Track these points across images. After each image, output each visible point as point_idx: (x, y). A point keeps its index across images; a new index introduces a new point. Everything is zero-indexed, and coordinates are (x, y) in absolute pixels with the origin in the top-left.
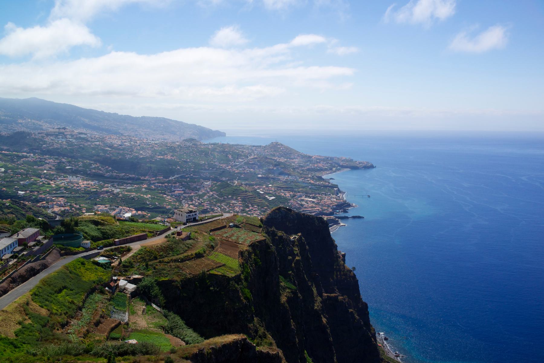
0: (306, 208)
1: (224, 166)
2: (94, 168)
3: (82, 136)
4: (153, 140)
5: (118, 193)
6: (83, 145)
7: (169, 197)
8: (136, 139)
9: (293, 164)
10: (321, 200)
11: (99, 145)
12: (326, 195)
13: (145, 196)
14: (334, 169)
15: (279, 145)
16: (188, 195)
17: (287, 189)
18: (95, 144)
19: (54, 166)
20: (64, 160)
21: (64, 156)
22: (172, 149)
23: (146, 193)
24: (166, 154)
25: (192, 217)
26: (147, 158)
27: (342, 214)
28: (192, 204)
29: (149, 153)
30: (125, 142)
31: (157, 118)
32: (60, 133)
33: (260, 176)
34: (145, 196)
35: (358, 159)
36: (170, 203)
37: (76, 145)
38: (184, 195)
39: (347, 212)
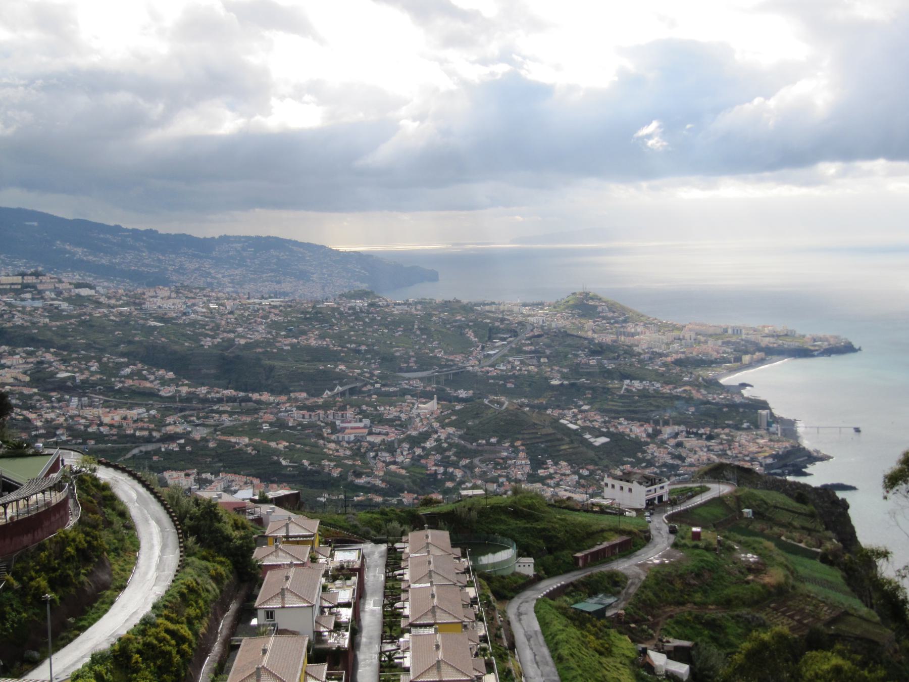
1: (458, 358)
2: (130, 376)
3: (85, 292)
4: (263, 298)
5: (204, 440)
6: (90, 314)
7: (333, 446)
8: (220, 294)
10: (730, 442)
11: (131, 313)
13: (273, 444)
14: (746, 359)
15: (592, 298)
17: (633, 415)
18: (121, 314)
19: (25, 373)
20: (49, 357)
21: (47, 345)
22: (316, 316)
23: (271, 436)
24: (304, 333)
26: (257, 344)
28: (395, 463)
29: (260, 333)
30: (194, 305)
32: (25, 287)
33: (555, 382)
34: (273, 444)
35: (807, 330)
36: (338, 461)
37: (70, 317)
38: (369, 438)
39: (805, 474)
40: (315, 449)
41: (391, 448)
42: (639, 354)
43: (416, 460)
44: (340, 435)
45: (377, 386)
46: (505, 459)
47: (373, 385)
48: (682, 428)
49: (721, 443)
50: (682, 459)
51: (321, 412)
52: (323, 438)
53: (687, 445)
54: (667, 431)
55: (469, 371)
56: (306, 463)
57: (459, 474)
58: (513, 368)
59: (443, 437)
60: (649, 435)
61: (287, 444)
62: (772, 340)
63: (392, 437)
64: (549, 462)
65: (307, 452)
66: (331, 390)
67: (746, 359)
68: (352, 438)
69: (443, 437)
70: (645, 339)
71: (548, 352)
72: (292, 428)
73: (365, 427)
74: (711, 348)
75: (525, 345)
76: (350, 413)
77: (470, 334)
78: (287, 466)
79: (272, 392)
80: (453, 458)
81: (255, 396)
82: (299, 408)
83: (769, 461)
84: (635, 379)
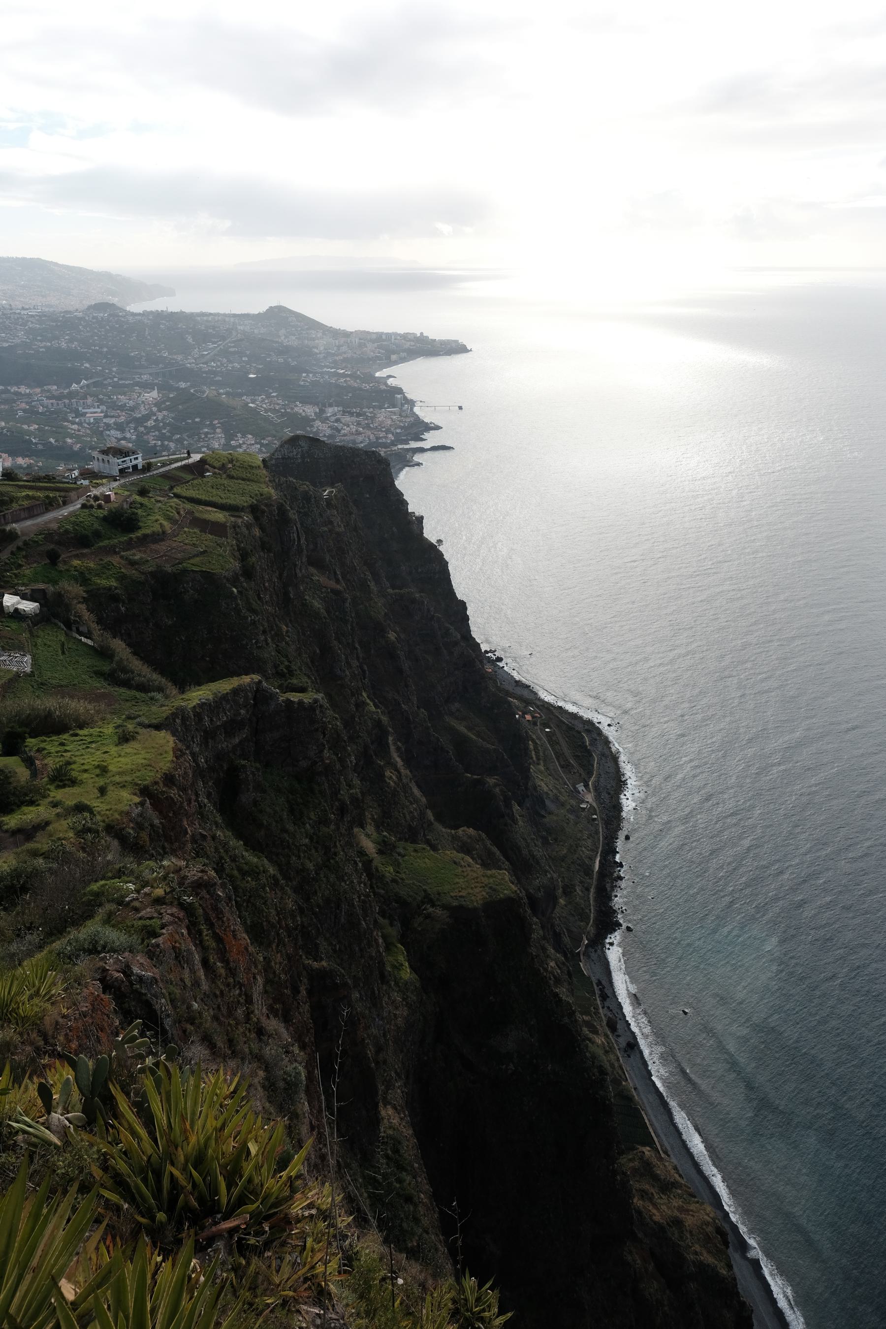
0: (345, 435)
1: (179, 357)
7: (75, 427)
9: (315, 350)
10: (373, 418)
12: (381, 408)
13: (25, 427)
14: (394, 357)
16: (113, 420)
25: (130, 465)
27: (414, 445)
28: (124, 438)
31: (24, 259)
34: (25, 427)
36: (78, 438)
38: (105, 420)
40: (60, 430)
41: (120, 427)
42: (317, 354)
43: (140, 436)
44: (82, 419)
45: (116, 379)
46: (206, 434)
47: (112, 379)
48: (340, 408)
49: (367, 419)
50: (339, 431)
51: (67, 401)
52: (68, 421)
53: (343, 421)
54: (330, 411)
55: (187, 368)
56: (52, 440)
57: (172, 445)
58: (222, 365)
59: (160, 418)
60: (316, 413)
61: (37, 427)
62: (412, 343)
63: (122, 419)
64: (239, 435)
65: (53, 432)
66: (78, 383)
67: (394, 357)
68: (92, 420)
69: (160, 418)
70: (322, 344)
71: (248, 352)
72: (41, 414)
73: (102, 412)
74: (370, 349)
75: (231, 347)
76: (89, 400)
77: (190, 339)
78: (36, 444)
79: (29, 386)
80: (168, 434)
81: (14, 389)
82: (48, 398)
83: (398, 431)
84: (311, 372)
